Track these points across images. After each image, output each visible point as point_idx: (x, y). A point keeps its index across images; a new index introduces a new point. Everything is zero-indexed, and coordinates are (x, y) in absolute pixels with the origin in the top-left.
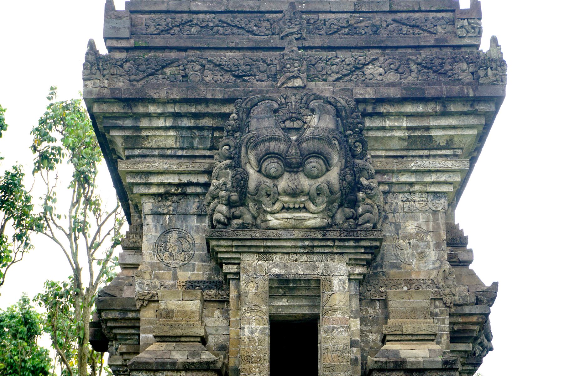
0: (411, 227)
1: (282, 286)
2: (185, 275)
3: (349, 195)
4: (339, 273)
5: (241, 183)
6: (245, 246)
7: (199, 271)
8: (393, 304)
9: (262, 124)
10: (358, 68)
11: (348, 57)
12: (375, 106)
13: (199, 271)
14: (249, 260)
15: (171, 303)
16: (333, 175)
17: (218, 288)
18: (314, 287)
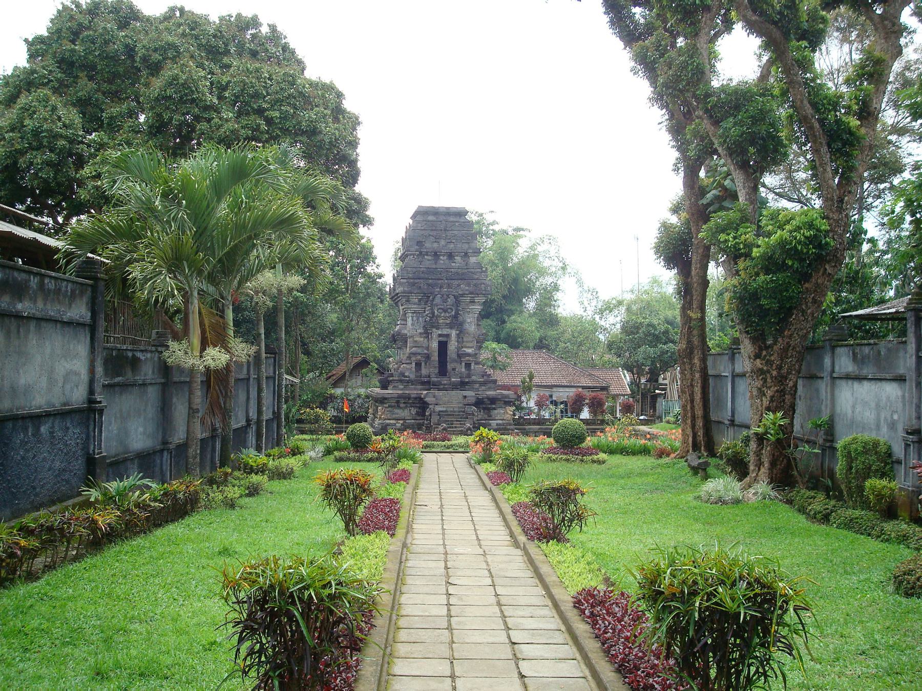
0: (469, 320)
1: (440, 335)
2: (419, 331)
3: (456, 317)
4: (454, 333)
5: (433, 313)
6: (433, 327)
7: (421, 331)
8: (465, 339)
9: (438, 300)
10: (459, 285)
11: (456, 282)
12: (462, 295)
13: (421, 331)
14: (434, 330)
15: (417, 339)
16: (453, 313)
17: (427, 334)
18: (448, 336)
